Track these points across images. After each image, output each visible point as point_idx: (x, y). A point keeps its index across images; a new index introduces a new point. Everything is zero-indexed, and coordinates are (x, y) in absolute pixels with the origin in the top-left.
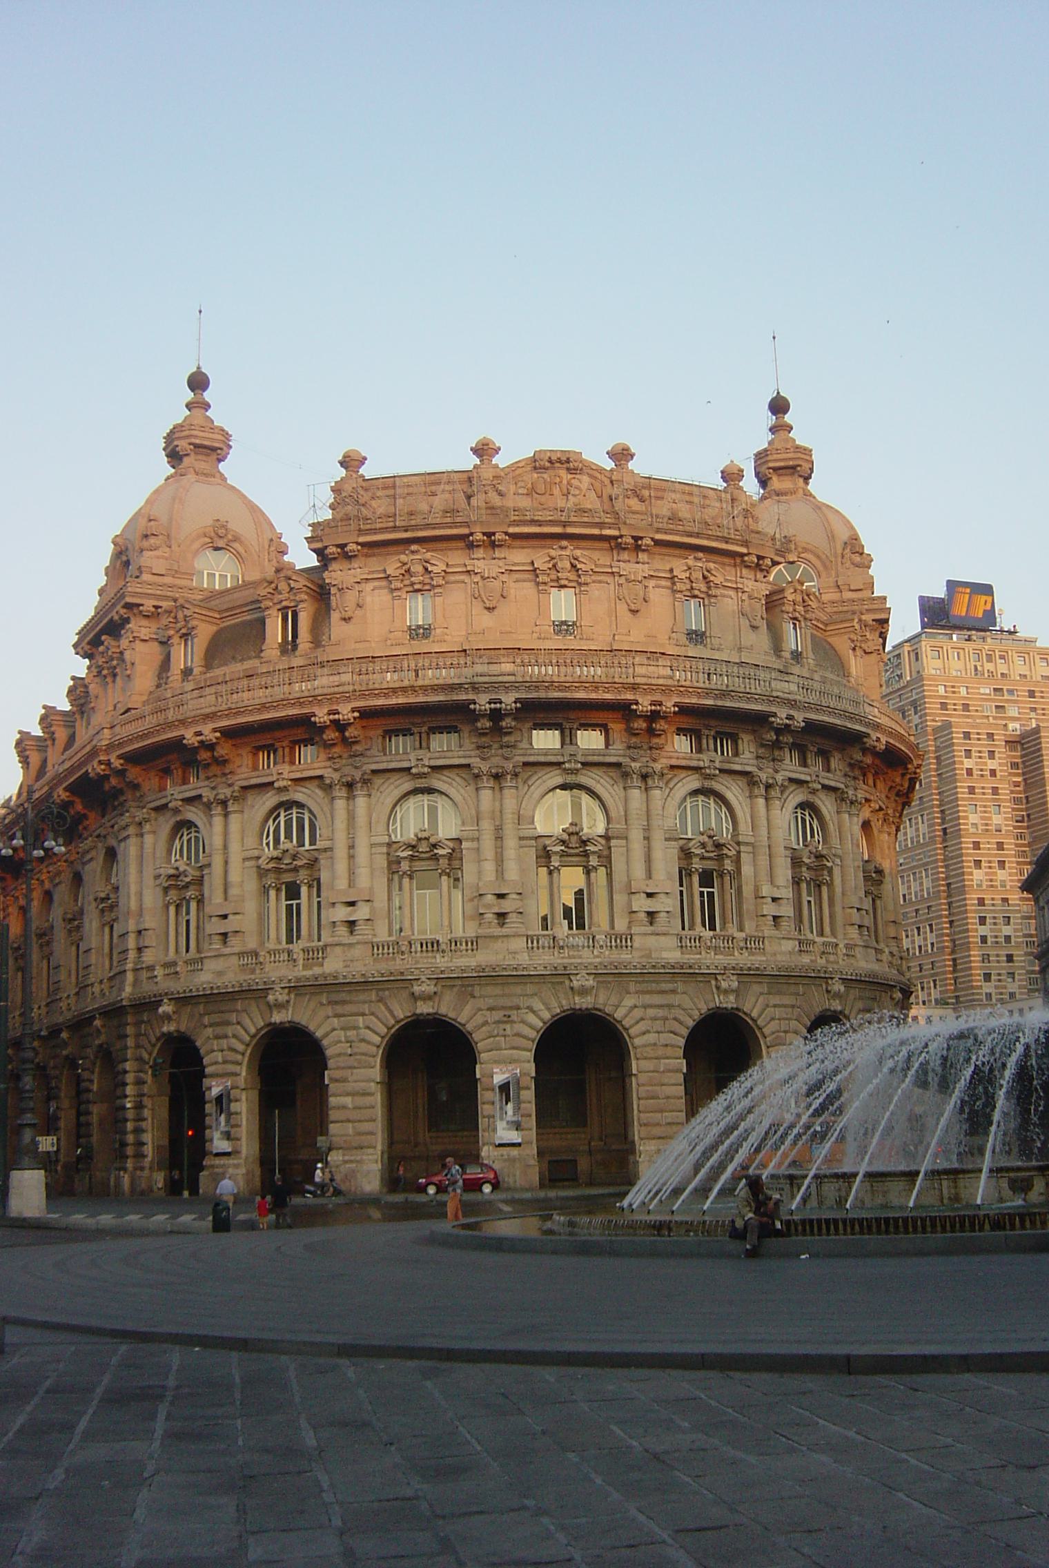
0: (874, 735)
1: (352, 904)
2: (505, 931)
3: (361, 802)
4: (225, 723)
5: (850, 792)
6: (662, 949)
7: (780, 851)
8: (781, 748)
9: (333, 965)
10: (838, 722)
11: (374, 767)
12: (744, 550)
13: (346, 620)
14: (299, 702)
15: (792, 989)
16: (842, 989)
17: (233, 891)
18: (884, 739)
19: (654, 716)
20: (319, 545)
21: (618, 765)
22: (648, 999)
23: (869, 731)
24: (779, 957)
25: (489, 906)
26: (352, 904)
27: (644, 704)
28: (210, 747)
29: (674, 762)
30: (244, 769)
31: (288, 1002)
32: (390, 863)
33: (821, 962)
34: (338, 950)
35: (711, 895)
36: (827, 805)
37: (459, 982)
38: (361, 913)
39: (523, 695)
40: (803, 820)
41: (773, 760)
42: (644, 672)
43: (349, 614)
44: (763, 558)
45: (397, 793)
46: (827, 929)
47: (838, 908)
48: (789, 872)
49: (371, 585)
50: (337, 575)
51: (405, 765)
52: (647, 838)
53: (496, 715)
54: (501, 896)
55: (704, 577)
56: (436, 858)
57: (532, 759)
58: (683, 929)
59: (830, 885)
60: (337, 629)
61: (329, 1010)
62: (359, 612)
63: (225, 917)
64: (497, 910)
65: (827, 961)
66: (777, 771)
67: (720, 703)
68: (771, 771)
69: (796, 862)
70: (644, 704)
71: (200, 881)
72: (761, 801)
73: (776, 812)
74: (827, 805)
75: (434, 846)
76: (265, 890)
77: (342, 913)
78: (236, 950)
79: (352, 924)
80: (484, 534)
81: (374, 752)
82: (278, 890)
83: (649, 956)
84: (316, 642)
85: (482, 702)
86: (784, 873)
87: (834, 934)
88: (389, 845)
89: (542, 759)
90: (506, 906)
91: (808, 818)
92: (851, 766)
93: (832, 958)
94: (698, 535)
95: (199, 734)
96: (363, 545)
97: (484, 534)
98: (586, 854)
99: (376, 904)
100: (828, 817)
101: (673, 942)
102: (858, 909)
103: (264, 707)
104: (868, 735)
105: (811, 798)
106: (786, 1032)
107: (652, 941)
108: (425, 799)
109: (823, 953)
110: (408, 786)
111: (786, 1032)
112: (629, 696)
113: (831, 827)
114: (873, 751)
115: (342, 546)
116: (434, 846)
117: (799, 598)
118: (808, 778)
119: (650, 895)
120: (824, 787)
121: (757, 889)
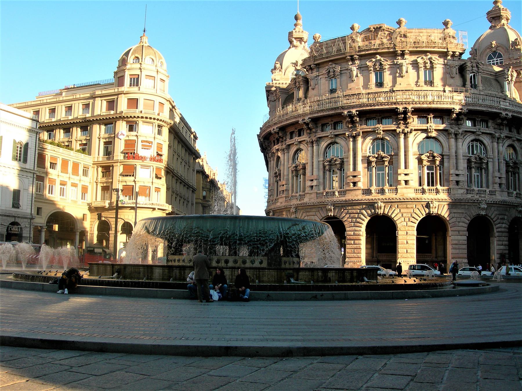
0: (504, 113)
1: (312, 180)
2: (355, 188)
3: (315, 147)
4: (279, 125)
5: (497, 135)
6: (408, 193)
7: (461, 157)
8: (461, 120)
9: (306, 200)
10: (484, 109)
11: (318, 136)
12: (446, 50)
13: (313, 89)
14: (295, 117)
15: (463, 207)
16: (486, 206)
17: (285, 177)
18: (510, 114)
19: (405, 112)
20: (304, 66)
21: (395, 130)
22: (402, 210)
23: (502, 112)
24: (456, 195)
25: (350, 180)
26: (312, 180)
27: (401, 108)
28: (278, 133)
29: (416, 128)
30: (288, 139)
31: (296, 212)
32: (324, 167)
33: (477, 197)
34: (308, 195)
35: (432, 174)
36: (486, 140)
37: (340, 205)
38: (315, 183)
39: (358, 109)
40: (477, 146)
41: (458, 125)
42: (399, 97)
43: (314, 87)
44: (455, 52)
45: (326, 144)
46: (484, 185)
47: (490, 178)
48: (466, 165)
49: (319, 78)
50: (311, 75)
51: (327, 135)
52: (405, 155)
53: (351, 116)
54: (355, 176)
55: (431, 62)
56: (336, 165)
57: (365, 130)
58: (420, 185)
59: (487, 169)
60: (311, 92)
61: (304, 214)
62: (317, 86)
63: (283, 185)
64: (352, 181)
65: (480, 197)
66: (459, 129)
67: (429, 106)
68: (457, 128)
69: (469, 161)
70: (401, 108)
71: (280, 174)
72: (453, 141)
73: (460, 144)
74: (486, 140)
75: (336, 161)
76: (293, 177)
77: (308, 183)
78: (284, 196)
79: (312, 187)
80: (350, 56)
81: (319, 131)
82: (297, 176)
83: (403, 195)
84: (306, 97)
85: (346, 112)
86: (463, 164)
87: (488, 187)
88: (323, 161)
89: (369, 130)
90: (356, 179)
91: (479, 145)
92: (500, 125)
93: (483, 195)
94: (426, 47)
95: (274, 129)
96: (316, 65)
97: (350, 56)
98: (384, 161)
99: (320, 180)
100: (486, 144)
101: (412, 191)
102: (500, 178)
103: (287, 120)
104: (501, 113)
105: (477, 137)
106: (459, 222)
107: (404, 191)
108: (336, 146)
109: (477, 194)
110: (329, 142)
111: (459, 222)
112: (394, 106)
113: (488, 148)
114: (505, 119)
115: (310, 66)
116: (336, 161)
117: (475, 65)
118: (475, 130)
119: (406, 175)
120: (483, 133)
121: (449, 172)
